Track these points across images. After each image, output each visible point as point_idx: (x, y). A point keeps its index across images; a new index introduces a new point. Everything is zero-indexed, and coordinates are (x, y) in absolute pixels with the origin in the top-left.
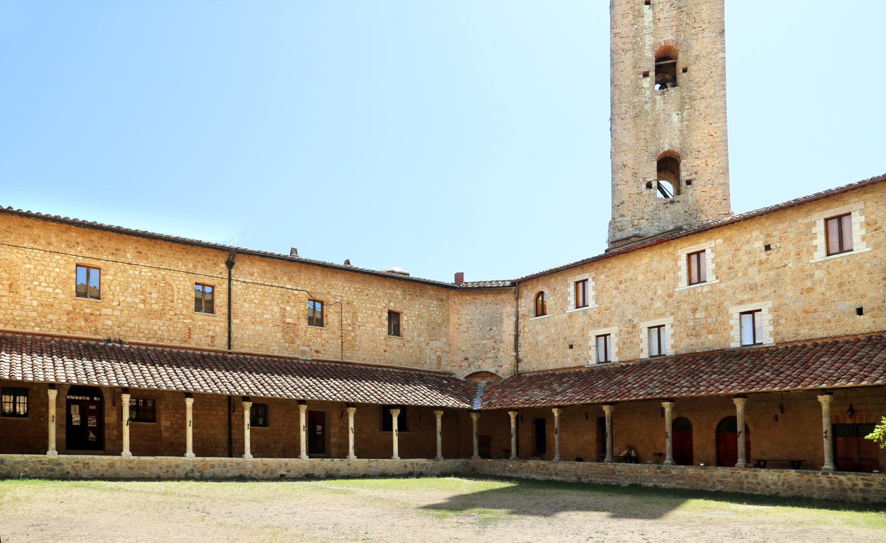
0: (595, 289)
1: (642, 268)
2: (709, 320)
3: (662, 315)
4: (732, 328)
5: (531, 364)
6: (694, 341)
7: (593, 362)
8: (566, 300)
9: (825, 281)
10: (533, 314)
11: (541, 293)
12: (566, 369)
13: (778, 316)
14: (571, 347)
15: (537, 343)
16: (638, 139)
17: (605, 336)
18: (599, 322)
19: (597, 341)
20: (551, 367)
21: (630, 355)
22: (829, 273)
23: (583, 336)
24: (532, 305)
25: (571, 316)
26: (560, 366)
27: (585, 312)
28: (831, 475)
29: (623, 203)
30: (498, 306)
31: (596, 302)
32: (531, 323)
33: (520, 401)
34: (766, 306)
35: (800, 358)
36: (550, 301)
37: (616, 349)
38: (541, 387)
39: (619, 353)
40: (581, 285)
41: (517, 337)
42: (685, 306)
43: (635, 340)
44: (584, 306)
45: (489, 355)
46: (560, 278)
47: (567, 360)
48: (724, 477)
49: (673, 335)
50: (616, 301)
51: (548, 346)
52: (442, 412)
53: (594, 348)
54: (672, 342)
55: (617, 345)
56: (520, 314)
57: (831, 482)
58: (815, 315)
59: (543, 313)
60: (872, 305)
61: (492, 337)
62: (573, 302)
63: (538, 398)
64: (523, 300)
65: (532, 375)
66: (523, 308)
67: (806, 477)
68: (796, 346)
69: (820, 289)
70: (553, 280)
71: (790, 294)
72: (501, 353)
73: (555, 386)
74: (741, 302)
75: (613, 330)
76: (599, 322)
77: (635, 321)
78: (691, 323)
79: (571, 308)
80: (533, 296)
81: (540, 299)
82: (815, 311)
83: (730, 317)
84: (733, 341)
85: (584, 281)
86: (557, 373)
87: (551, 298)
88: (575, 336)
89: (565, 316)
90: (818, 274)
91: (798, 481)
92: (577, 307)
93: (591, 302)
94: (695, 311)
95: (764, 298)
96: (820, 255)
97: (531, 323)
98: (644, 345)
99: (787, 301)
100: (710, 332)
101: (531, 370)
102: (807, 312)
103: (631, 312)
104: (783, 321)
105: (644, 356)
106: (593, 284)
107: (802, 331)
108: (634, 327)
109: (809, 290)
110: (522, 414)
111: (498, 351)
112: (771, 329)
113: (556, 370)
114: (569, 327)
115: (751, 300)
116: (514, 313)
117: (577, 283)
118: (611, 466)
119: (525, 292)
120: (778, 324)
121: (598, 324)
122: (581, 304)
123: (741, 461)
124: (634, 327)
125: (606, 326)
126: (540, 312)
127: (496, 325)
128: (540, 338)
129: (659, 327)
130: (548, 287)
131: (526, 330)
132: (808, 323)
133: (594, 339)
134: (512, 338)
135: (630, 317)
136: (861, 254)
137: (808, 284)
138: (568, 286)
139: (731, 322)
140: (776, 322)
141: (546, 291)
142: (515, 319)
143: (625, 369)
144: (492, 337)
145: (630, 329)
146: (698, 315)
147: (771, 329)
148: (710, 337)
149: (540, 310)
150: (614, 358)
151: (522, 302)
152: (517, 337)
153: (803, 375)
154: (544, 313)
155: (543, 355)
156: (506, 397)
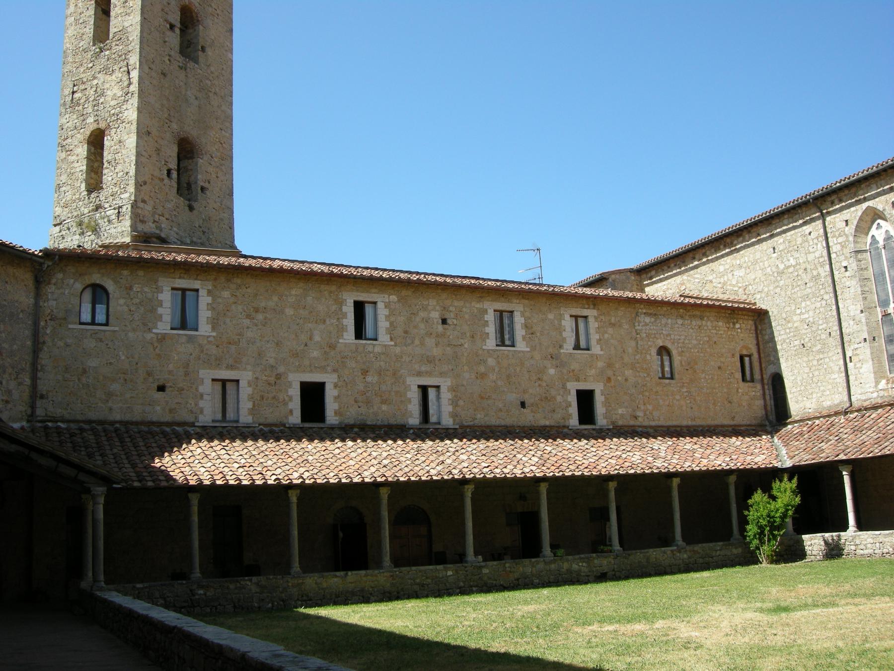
0: (211, 307)
1: (292, 300)
2: (384, 388)
3: (323, 369)
4: (410, 401)
6: (363, 410)
8: (153, 310)
9: (497, 369)
13: (456, 396)
16: (162, 105)
21: (271, 415)
22: (498, 363)
23: (187, 374)
25: (162, 338)
26: (137, 418)
27: (190, 339)
29: (145, 183)
30: (9, 287)
31: (213, 329)
34: (445, 384)
36: (119, 303)
37: (250, 405)
39: (252, 411)
42: (351, 364)
43: (281, 396)
46: (141, 273)
49: (336, 398)
50: (249, 334)
52: (298, 491)
54: (336, 406)
55: (251, 397)
58: (489, 402)
60: (532, 401)
62: (167, 318)
64: (51, 289)
69: (493, 377)
70: (125, 272)
71: (467, 375)
74: (419, 374)
75: (245, 376)
77: (281, 369)
78: (361, 387)
79: (163, 327)
82: (489, 398)
83: (408, 388)
84: (411, 416)
87: (122, 301)
88: (170, 372)
89: (149, 336)
90: (491, 362)
93: (205, 329)
94: (365, 372)
95: (442, 374)
96: (491, 343)
99: (465, 383)
100: (384, 402)
102: (482, 398)
103: (273, 355)
104: (461, 403)
106: (209, 300)
107: (479, 416)
108: (279, 376)
109: (483, 376)
112: (450, 408)
114: (159, 355)
115: (429, 374)
120: (457, 405)
121: (218, 363)
123: (547, 550)
124: (279, 376)
125: (230, 367)
128: (92, 363)
130: (116, 282)
132: (483, 409)
135: (272, 361)
136: (523, 352)
137: (482, 369)
138: (159, 290)
139: (409, 395)
140: (454, 402)
141: (110, 286)
145: (272, 380)
146: (369, 379)
147: (450, 408)
148: (384, 407)
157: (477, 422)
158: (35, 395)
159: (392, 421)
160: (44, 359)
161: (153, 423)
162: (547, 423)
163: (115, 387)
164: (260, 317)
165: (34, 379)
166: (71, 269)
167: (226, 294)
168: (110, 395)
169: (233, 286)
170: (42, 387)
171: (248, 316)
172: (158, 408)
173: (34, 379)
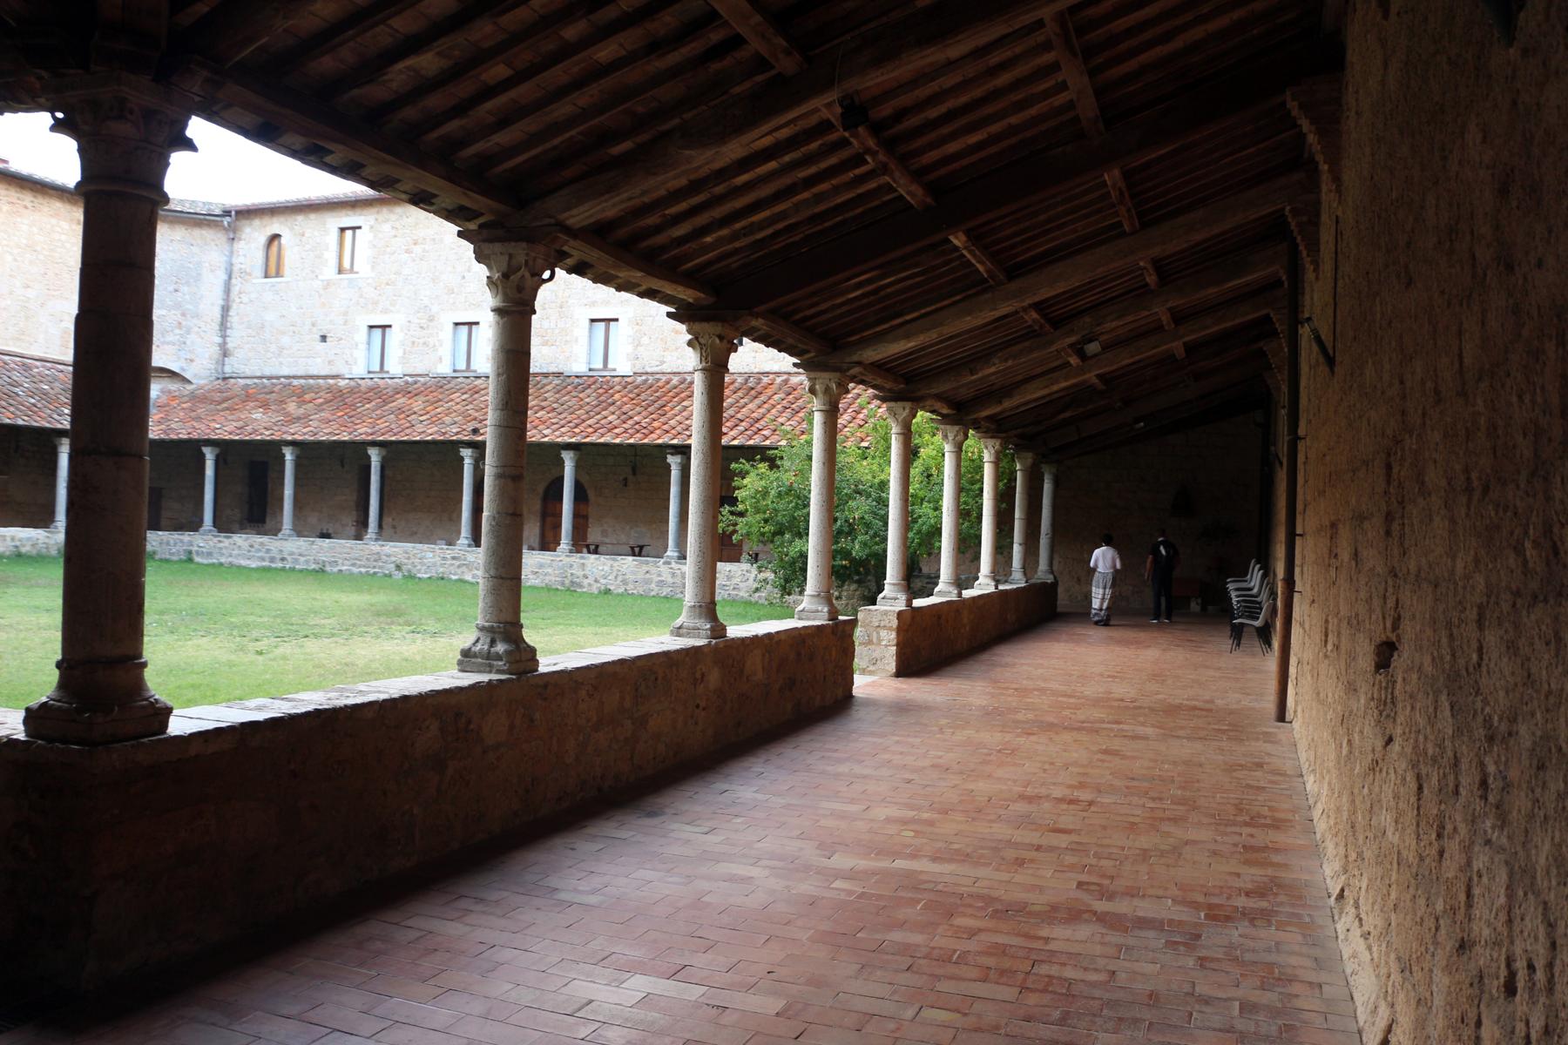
5: (250, 362)
7: (359, 370)
10: (259, 272)
11: (275, 237)
12: (311, 377)
14: (324, 338)
15: (263, 327)
17: (384, 327)
18: (376, 303)
19: (369, 335)
20: (286, 372)
21: (419, 365)
23: (345, 323)
24: (259, 256)
25: (328, 284)
28: (674, 565)
31: (373, 268)
32: (253, 288)
33: (225, 428)
35: (659, 398)
37: (400, 353)
38: (265, 405)
40: (349, 233)
41: (226, 309)
44: (352, 270)
45: (170, 338)
46: (313, 216)
47: (314, 362)
48: (541, 566)
51: (283, 333)
53: (363, 347)
56: (236, 269)
57: (673, 575)
59: (278, 274)
61: (178, 306)
63: (259, 425)
65: (249, 382)
66: (241, 259)
67: (645, 568)
68: (658, 380)
72: (192, 337)
73: (292, 407)
74: (593, 304)
76: (376, 303)
77: (435, 309)
79: (330, 271)
80: (262, 239)
81: (274, 248)
85: (354, 229)
86: (295, 382)
88: (331, 322)
91: (633, 573)
92: (340, 271)
97: (253, 288)
98: (445, 351)
101: (249, 373)
104: (645, 340)
105: (445, 369)
108: (431, 319)
110: (228, 450)
111: (188, 332)
112: (630, 349)
113: (294, 377)
115: (607, 303)
116: (223, 266)
117: (343, 230)
118: (375, 547)
119: (248, 230)
122: (347, 265)
125: (385, 311)
126: (273, 270)
127: (188, 283)
129: (470, 324)
130: (292, 229)
131: (245, 299)
133: (365, 329)
134: (216, 313)
142: (225, 277)
143: (410, 388)
144: (178, 306)
149: (273, 268)
150: (395, 367)
151: (240, 246)
152: (226, 309)
153: (656, 424)
154: (278, 274)
155: (273, 348)
156: (198, 419)
157: (666, 368)
158: (225, 353)
159: (553, 369)
160: (234, 318)
161: (318, 377)
162: (776, 368)
163: (285, 340)
164: (418, 249)
165: (224, 337)
166: (257, 222)
167: (386, 227)
168: (282, 349)
169: (393, 217)
170: (230, 345)
171: (408, 251)
172: (319, 360)
173: (224, 337)
